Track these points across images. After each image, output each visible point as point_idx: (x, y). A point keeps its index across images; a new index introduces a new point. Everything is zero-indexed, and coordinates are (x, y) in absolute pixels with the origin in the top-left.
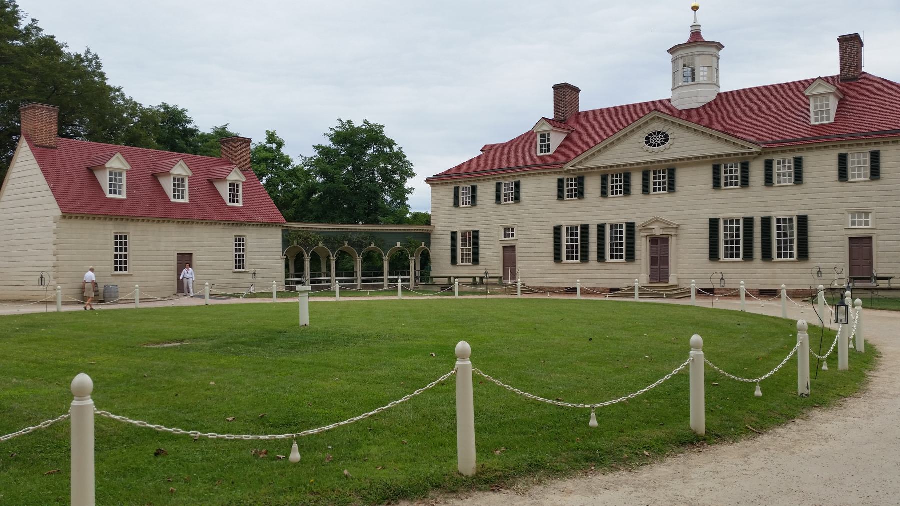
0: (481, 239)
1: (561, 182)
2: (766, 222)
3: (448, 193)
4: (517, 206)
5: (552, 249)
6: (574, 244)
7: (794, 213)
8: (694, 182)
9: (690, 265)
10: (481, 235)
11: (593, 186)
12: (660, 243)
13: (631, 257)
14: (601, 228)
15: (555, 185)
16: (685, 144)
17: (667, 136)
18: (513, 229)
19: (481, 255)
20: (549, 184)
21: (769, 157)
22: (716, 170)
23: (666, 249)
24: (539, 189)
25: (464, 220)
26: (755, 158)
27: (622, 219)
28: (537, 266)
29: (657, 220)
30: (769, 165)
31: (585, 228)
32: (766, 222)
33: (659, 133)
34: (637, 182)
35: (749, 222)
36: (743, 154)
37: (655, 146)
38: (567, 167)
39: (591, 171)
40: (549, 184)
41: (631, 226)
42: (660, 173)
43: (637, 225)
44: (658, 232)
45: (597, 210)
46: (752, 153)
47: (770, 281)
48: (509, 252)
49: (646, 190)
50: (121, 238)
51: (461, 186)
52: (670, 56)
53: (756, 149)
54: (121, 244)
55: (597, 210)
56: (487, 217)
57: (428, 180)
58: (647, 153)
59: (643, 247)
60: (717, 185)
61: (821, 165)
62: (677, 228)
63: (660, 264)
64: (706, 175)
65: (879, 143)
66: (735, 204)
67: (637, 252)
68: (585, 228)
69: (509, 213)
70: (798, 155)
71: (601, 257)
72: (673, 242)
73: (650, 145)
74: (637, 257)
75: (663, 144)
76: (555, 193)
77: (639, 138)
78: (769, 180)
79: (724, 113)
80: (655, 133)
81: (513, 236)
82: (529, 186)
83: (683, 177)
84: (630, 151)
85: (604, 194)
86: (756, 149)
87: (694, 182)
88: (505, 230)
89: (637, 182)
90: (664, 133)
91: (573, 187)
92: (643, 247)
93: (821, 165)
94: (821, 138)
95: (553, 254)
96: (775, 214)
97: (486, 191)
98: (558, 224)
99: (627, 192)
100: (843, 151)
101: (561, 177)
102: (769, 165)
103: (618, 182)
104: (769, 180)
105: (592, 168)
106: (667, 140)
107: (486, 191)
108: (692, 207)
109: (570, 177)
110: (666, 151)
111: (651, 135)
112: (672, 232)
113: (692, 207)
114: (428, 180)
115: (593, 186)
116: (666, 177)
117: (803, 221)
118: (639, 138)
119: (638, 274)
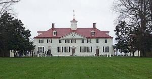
12: (74, 50)
14: (65, 47)
16: (77, 37)
25: (41, 45)
28: (54, 53)
31: (63, 47)
39: (63, 39)
55: (63, 44)
56: (45, 45)
61: (94, 41)
63: (73, 52)
69: (49, 45)
71: (65, 51)
79: (79, 31)
94: (93, 38)
97: (45, 41)
107: (45, 41)
113: (78, 45)
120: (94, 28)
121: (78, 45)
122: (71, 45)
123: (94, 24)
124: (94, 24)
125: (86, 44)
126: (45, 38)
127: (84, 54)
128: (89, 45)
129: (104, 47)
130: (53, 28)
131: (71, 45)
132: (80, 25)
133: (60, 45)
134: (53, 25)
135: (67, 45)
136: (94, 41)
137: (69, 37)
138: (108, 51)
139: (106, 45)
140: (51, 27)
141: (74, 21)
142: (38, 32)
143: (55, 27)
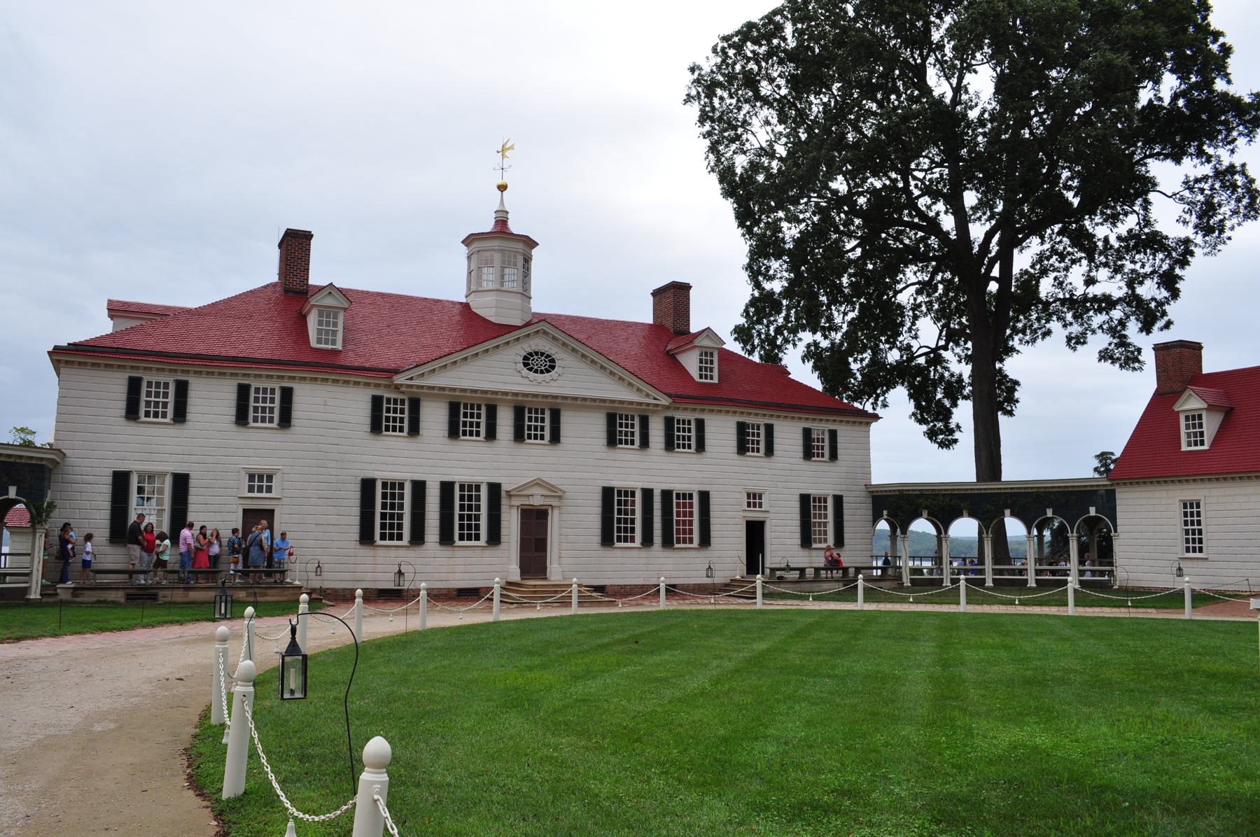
0: (192, 491)
2: (667, 495)
4: (282, 436)
5: (356, 520)
6: (382, 512)
7: (695, 488)
8: (584, 431)
9: (575, 552)
10: (192, 483)
11: (434, 417)
12: (535, 520)
13: (495, 537)
14: (447, 488)
17: (553, 361)
18: (270, 478)
19: (713, 534)
20: (352, 404)
21: (669, 414)
22: (611, 419)
24: (332, 412)
25: (154, 448)
26: (654, 412)
27: (483, 477)
29: (538, 483)
31: (419, 488)
33: (542, 354)
35: (648, 494)
36: (648, 405)
37: (536, 372)
38: (400, 379)
39: (437, 392)
40: (352, 404)
41: (495, 489)
42: (536, 413)
43: (504, 488)
44: (537, 501)
46: (657, 405)
47: (681, 574)
49: (519, 436)
50: (1192, 507)
51: (146, 378)
54: (1192, 515)
55: (431, 457)
58: (526, 381)
62: (560, 497)
64: (596, 426)
65: (188, 372)
67: (504, 531)
68: (419, 488)
69: (261, 446)
73: (530, 369)
74: (503, 538)
75: (548, 371)
76: (367, 420)
77: (516, 353)
80: (537, 353)
81: (269, 489)
82: (310, 398)
85: (454, 432)
86: (665, 401)
87: (584, 431)
88: (251, 477)
90: (548, 356)
91: (393, 415)
93: (721, 430)
95: (357, 529)
96: (677, 486)
97: (212, 399)
99: (491, 435)
101: (378, 392)
102: (669, 422)
103: (470, 417)
105: (433, 388)
106: (553, 367)
107: (212, 399)
108: (579, 467)
109: (392, 396)
110: (553, 383)
111: (530, 354)
112: (555, 502)
113: (579, 467)
115: (434, 417)
116: (538, 420)
117: (705, 497)
118: (516, 353)
119: (499, 565)
125: (651, 469)
126: (212, 364)
135: (472, 462)
137: (496, 373)
139: (822, 479)
143: (317, 277)
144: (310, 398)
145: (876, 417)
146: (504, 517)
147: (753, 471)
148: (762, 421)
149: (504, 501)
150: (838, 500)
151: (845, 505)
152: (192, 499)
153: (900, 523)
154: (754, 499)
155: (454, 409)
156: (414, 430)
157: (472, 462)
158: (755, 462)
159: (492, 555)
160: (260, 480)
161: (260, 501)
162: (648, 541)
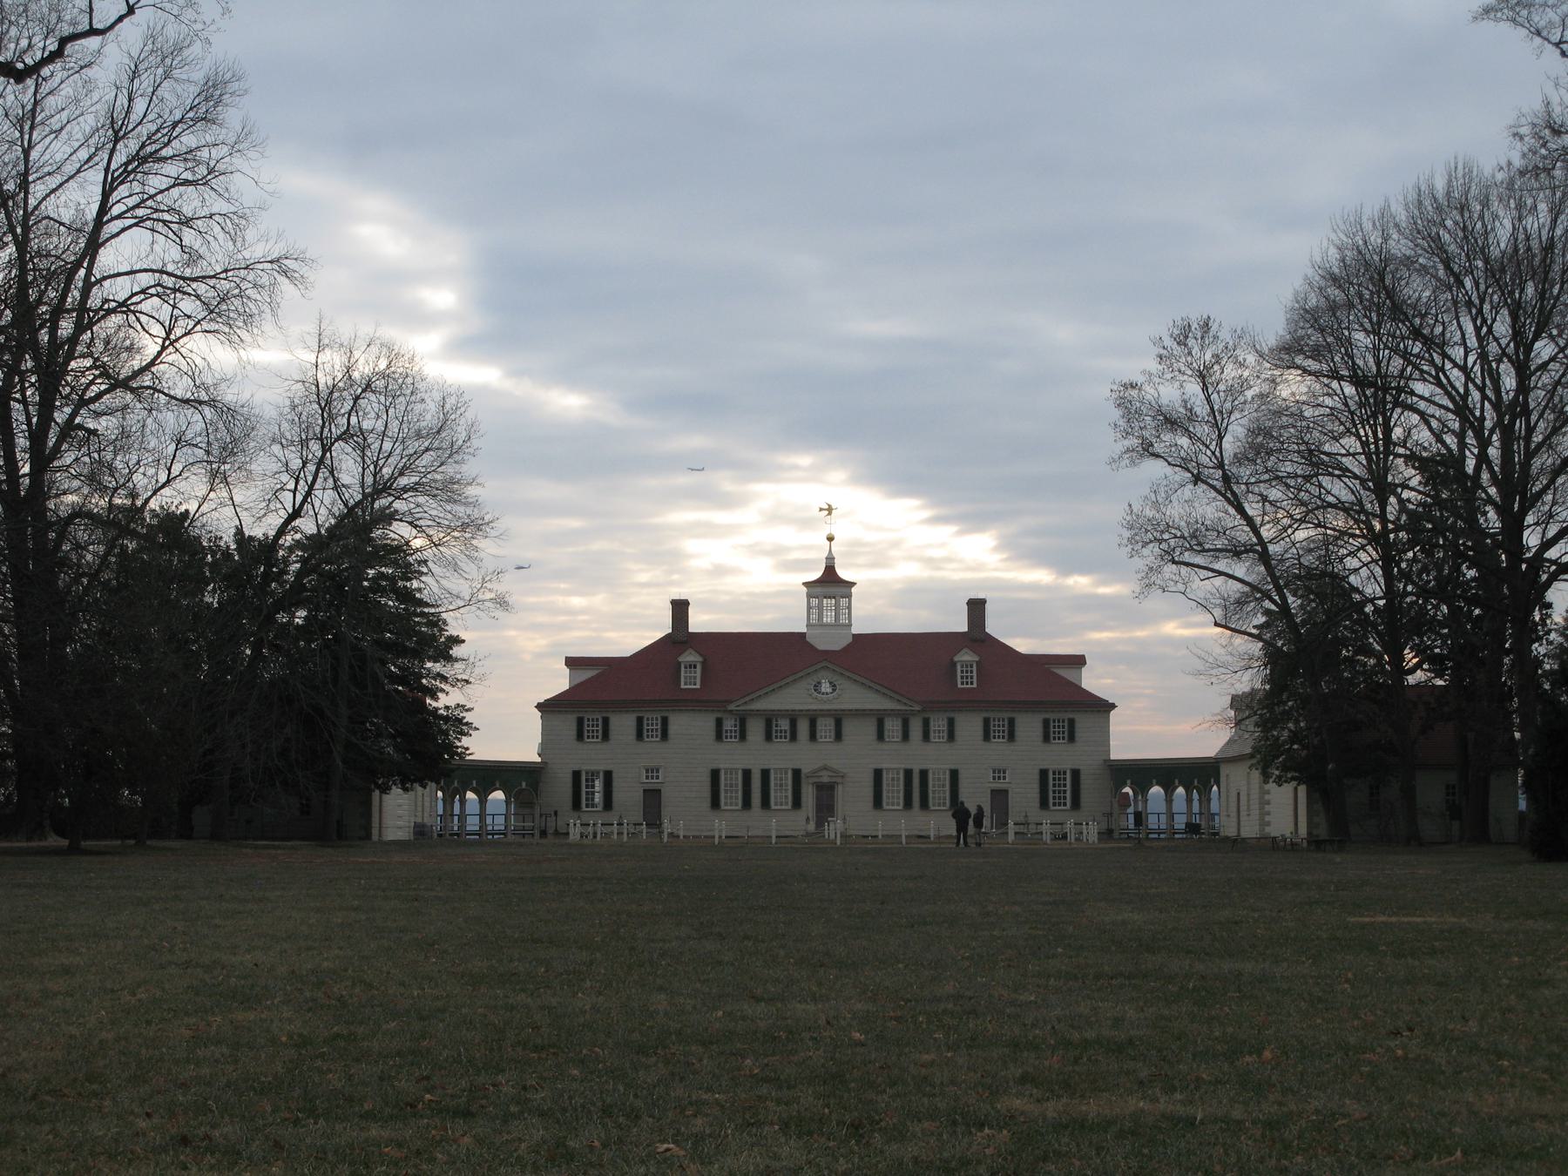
1: (719, 722)
3: (567, 724)
8: (859, 733)
9: (854, 815)
10: (614, 775)
11: (756, 729)
13: (797, 803)
14: (765, 774)
15: (712, 724)
23: (832, 797)
24: (691, 727)
25: (593, 757)
28: (686, 815)
29: (825, 768)
30: (926, 723)
31: (747, 774)
32: (924, 774)
34: (803, 728)
35: (908, 774)
38: (732, 707)
39: (758, 713)
41: (797, 774)
44: (825, 780)
45: (754, 754)
48: (653, 798)
49: (813, 736)
52: (805, 589)
53: (917, 708)
56: (624, 754)
57: (539, 706)
59: (809, 795)
60: (880, 736)
61: (970, 726)
63: (825, 808)
64: (870, 728)
66: (896, 757)
67: (804, 799)
69: (652, 752)
70: (952, 715)
72: (839, 790)
76: (713, 734)
78: (926, 736)
82: (678, 723)
83: (848, 727)
84: (793, 697)
86: (917, 708)
87: (859, 733)
89: (803, 728)
92: (809, 795)
94: (968, 702)
97: (623, 724)
98: (715, 766)
99: (794, 737)
100: (986, 715)
102: (926, 723)
104: (926, 736)
107: (623, 724)
114: (539, 706)
115: (756, 729)
117: (954, 775)
120: (977, 635)
121: (854, 758)
122: (806, 756)
123: (976, 608)
124: (976, 608)
126: (623, 706)
127: (898, 823)
128: (934, 757)
129: (1044, 774)
130: (680, 637)
131: (806, 756)
132: (872, 612)
133: (735, 757)
134: (680, 608)
135: (781, 757)
136: (970, 726)
138: (1076, 804)
139: (1060, 757)
140: (661, 627)
141: (830, 584)
142: (572, 663)
144: (680, 723)
145: (1113, 706)
146: (804, 790)
147: (998, 751)
148: (1006, 715)
149: (803, 781)
150: (1076, 774)
151: (1083, 777)
152: (615, 784)
153: (1142, 788)
154: (999, 773)
155: (769, 723)
156: (743, 737)
157: (781, 757)
158: (999, 747)
159: (800, 816)
160: (652, 771)
161: (653, 783)
162: (908, 804)
